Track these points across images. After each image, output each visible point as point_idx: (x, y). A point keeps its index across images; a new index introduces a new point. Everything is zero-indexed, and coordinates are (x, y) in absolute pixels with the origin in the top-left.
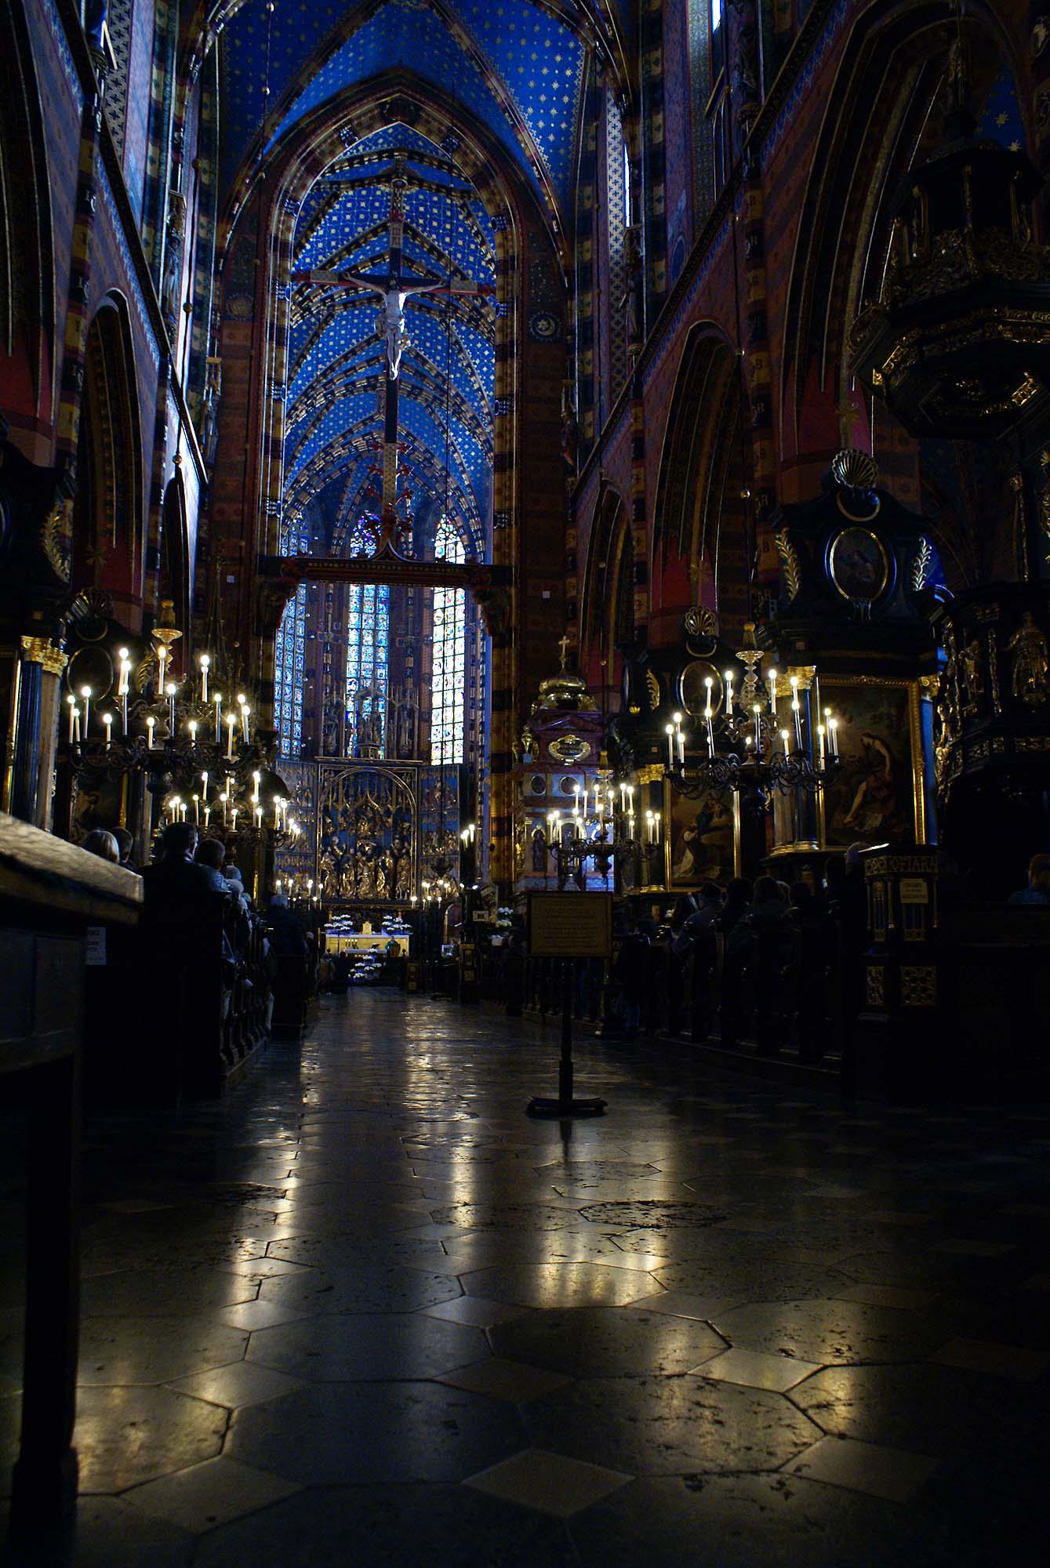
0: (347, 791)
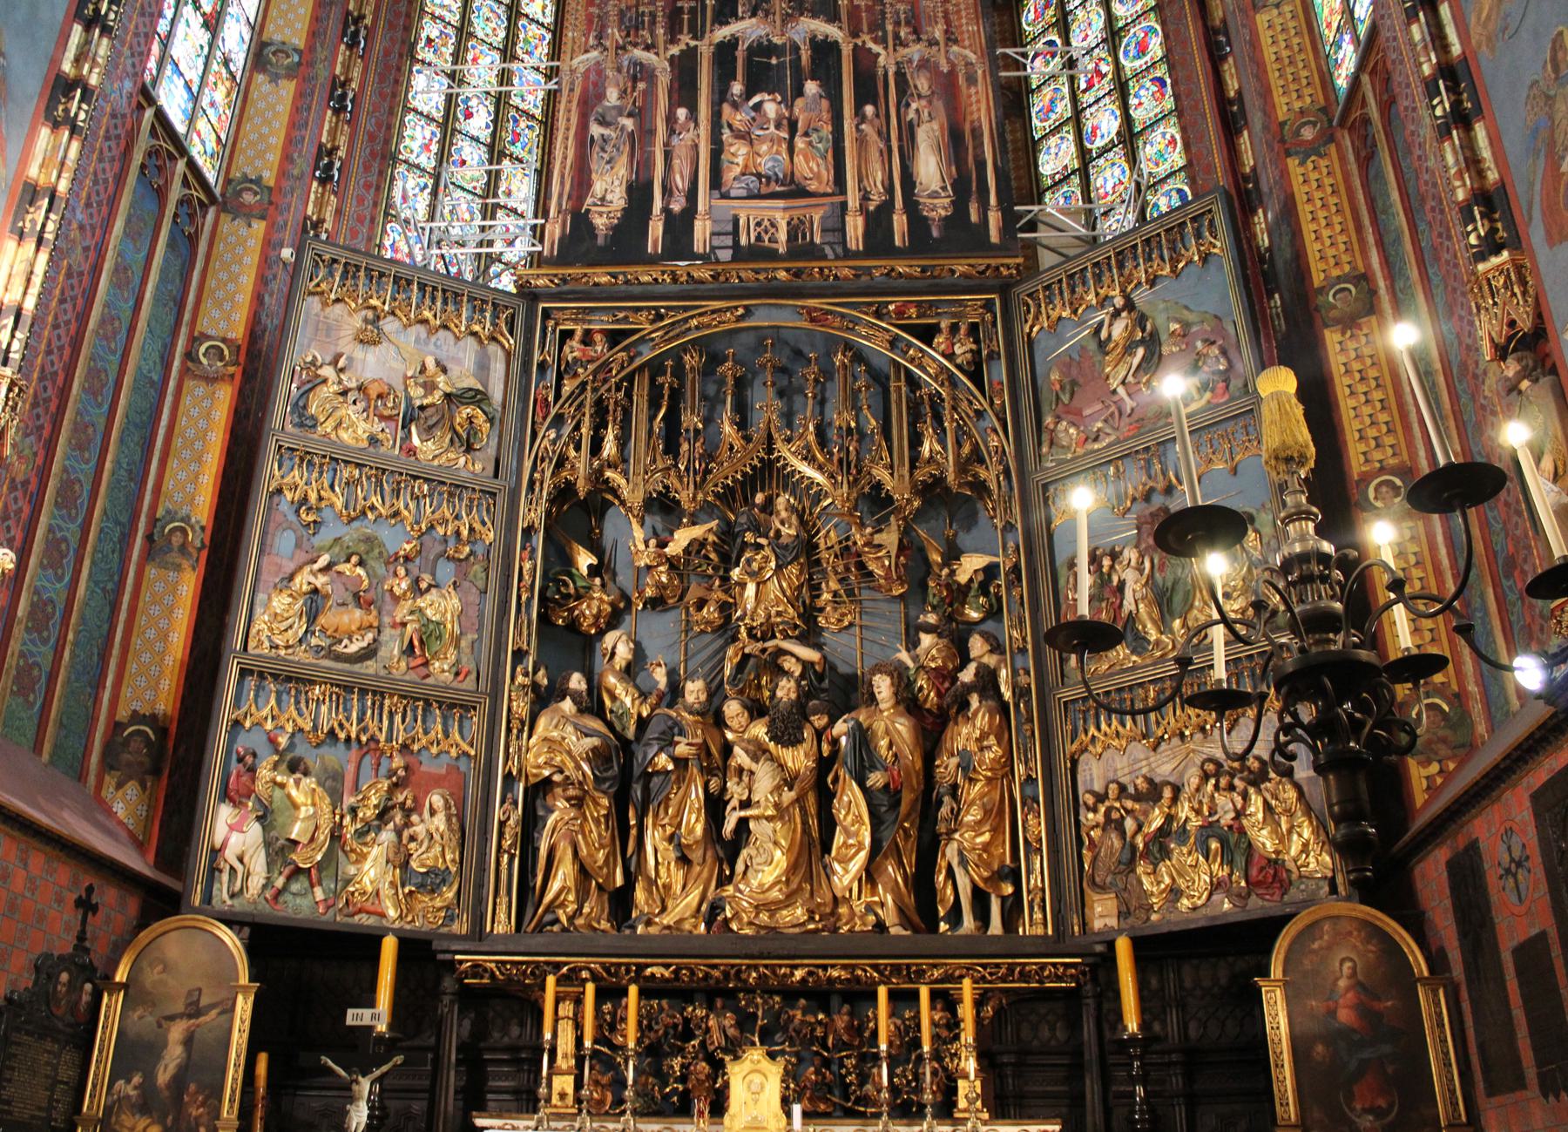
0: (672, 420)
